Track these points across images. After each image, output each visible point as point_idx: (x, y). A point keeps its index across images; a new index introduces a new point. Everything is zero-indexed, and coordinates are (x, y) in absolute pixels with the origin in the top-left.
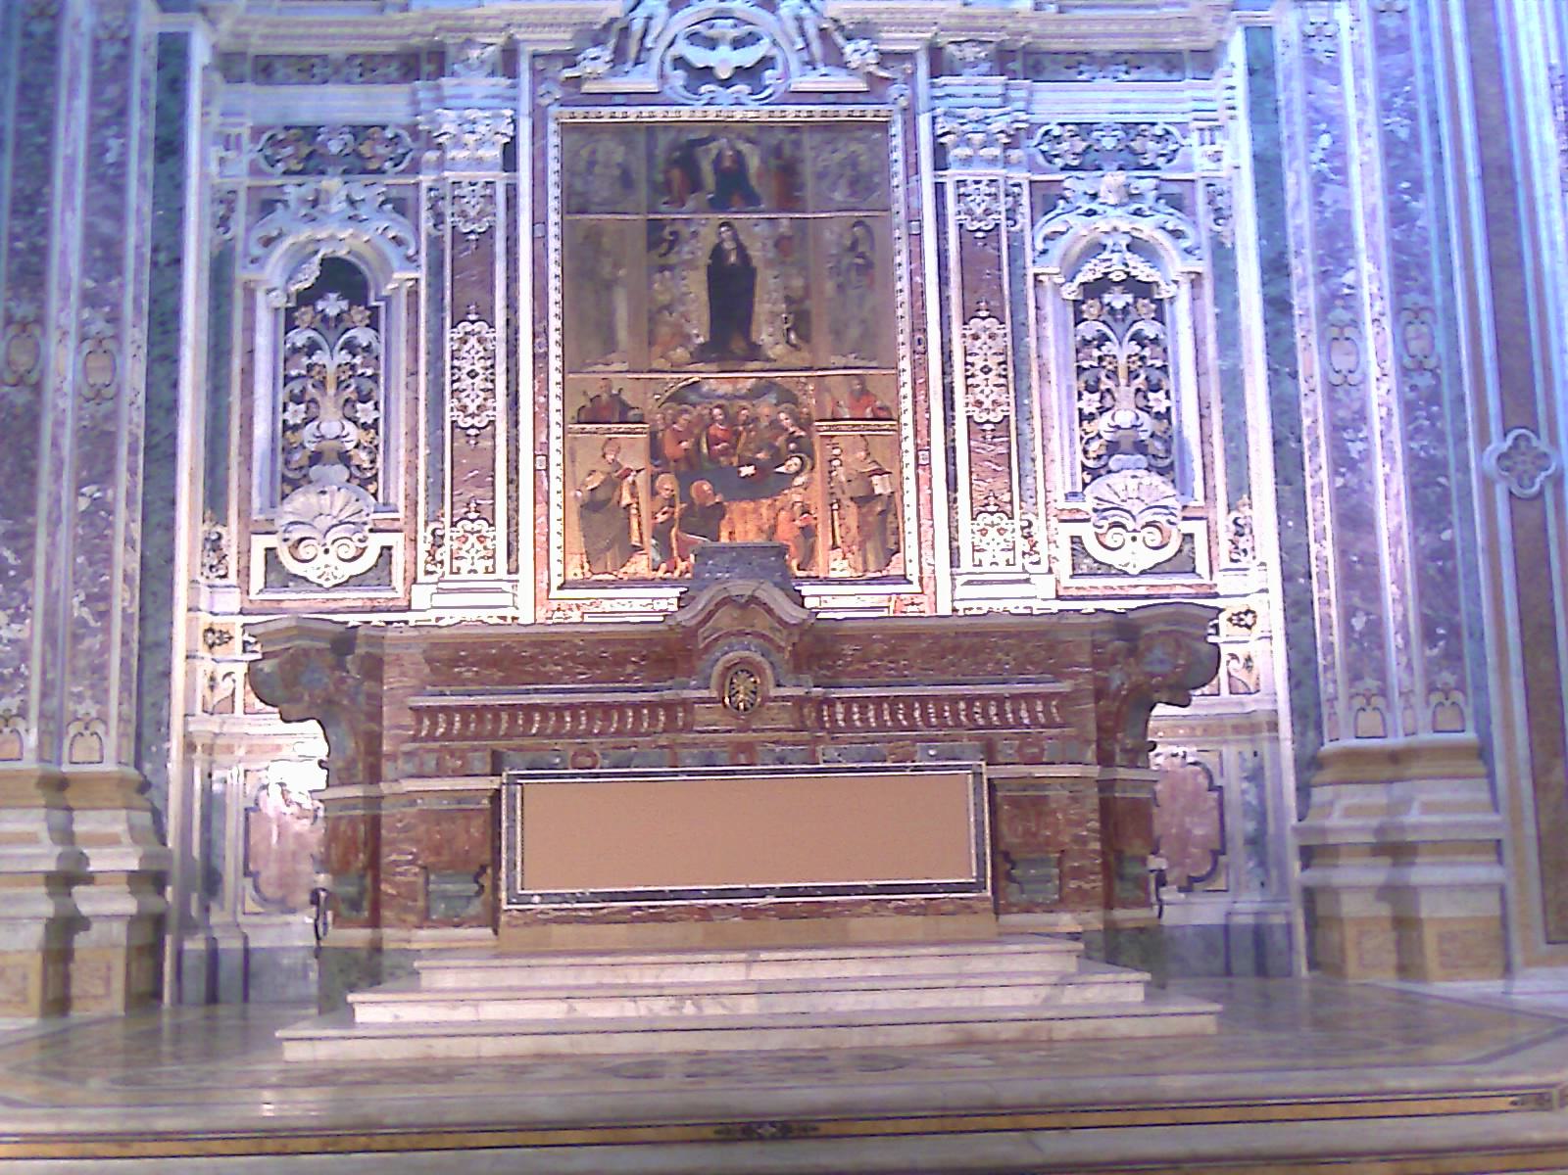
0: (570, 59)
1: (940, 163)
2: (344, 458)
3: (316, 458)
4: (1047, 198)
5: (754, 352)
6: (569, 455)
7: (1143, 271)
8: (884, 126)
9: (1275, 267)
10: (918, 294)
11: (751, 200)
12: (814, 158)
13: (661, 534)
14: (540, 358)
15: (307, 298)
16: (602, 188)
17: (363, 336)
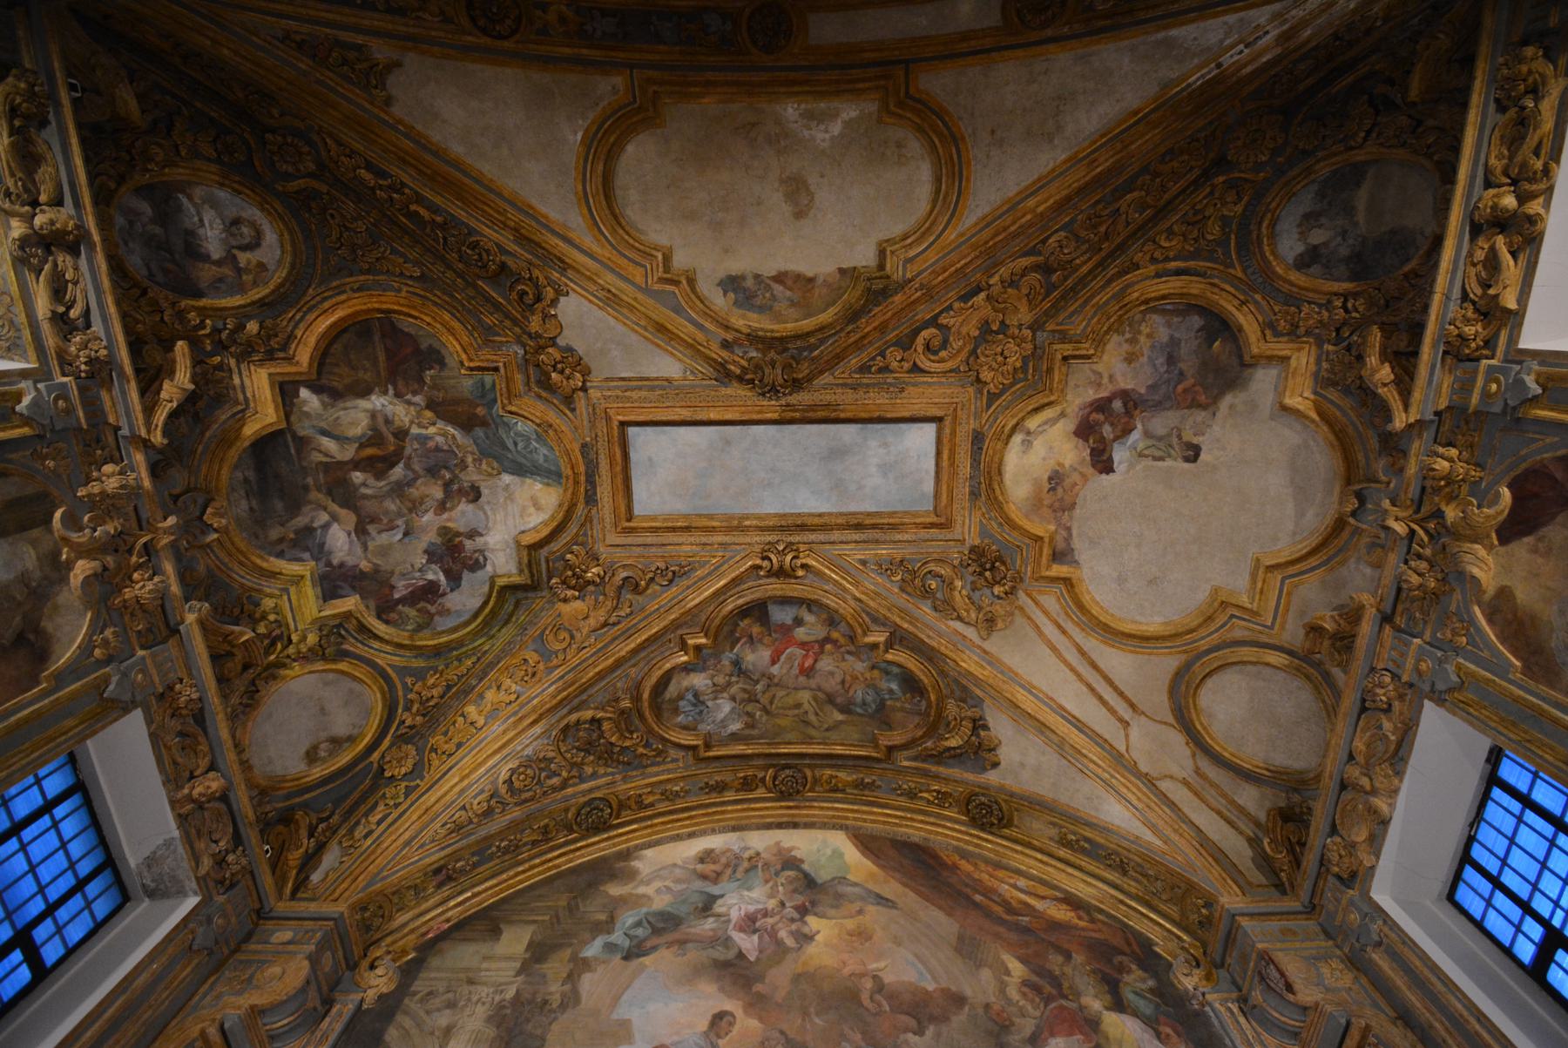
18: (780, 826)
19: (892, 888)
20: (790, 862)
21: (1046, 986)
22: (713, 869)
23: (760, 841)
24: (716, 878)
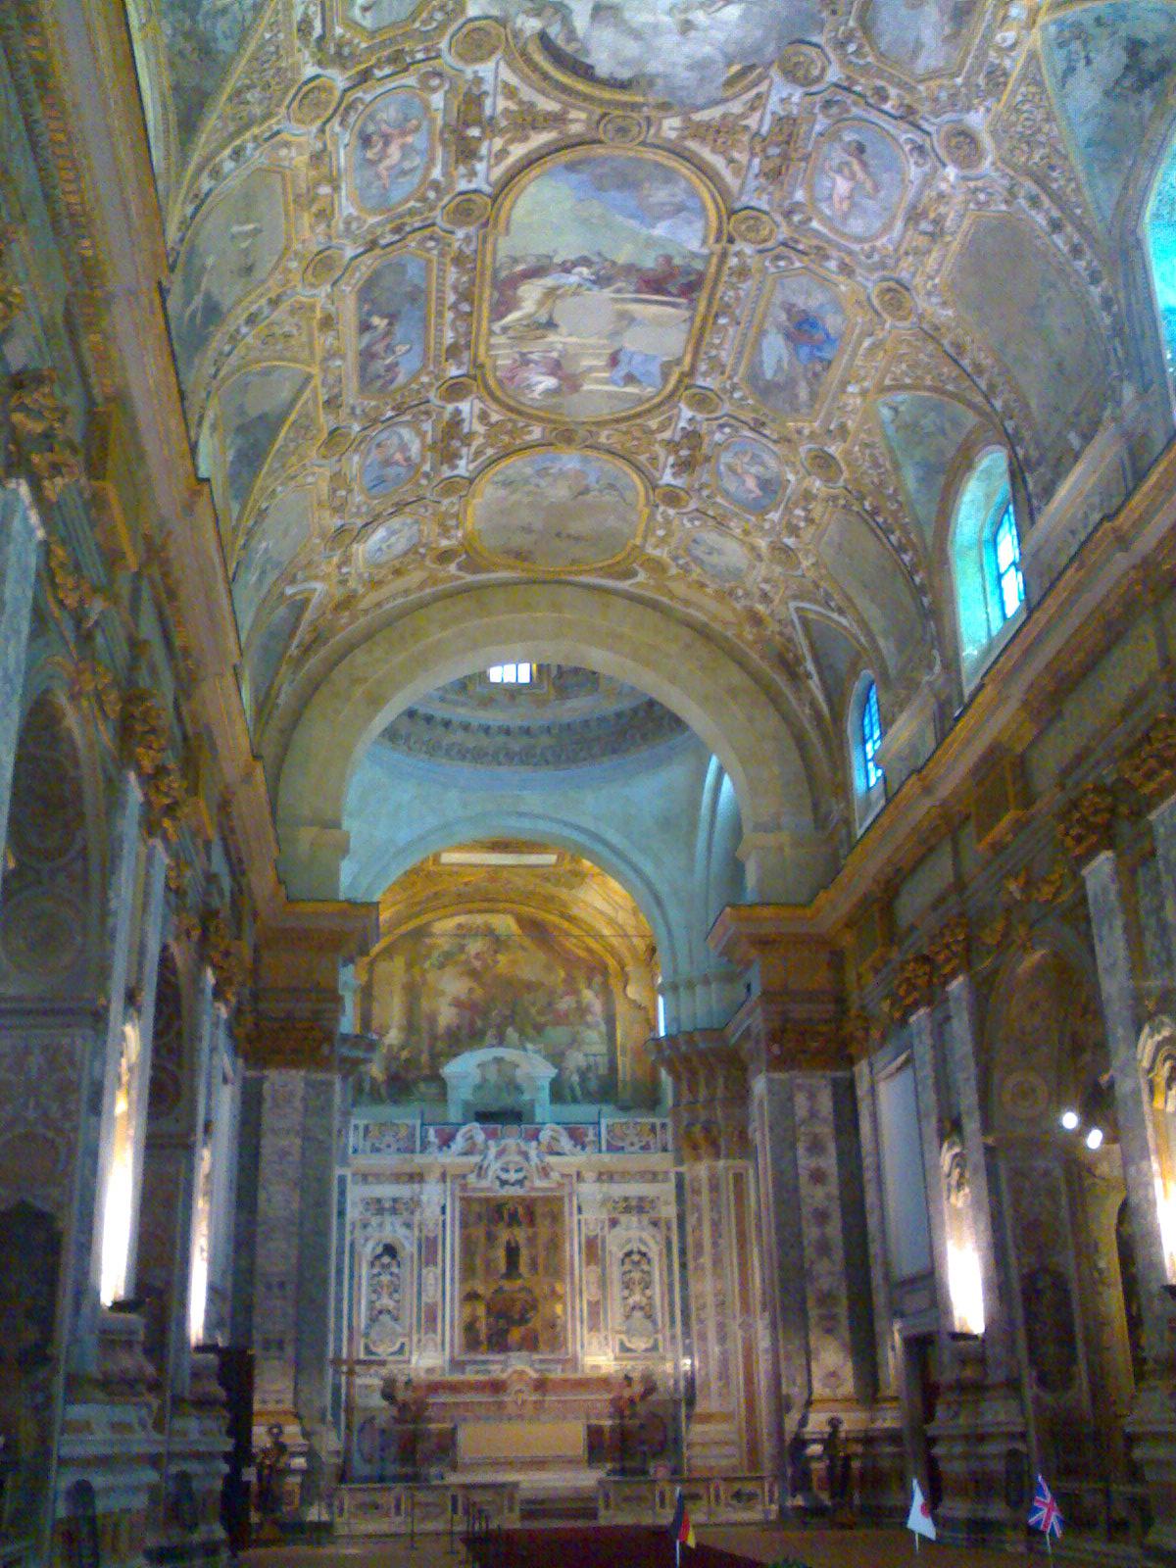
3: (380, 1312)
4: (614, 1223)
5: (520, 1276)
7: (644, 1249)
9: (683, 1252)
11: (519, 1224)
12: (539, 1210)
13: (489, 1338)
15: (378, 1257)
16: (472, 1219)
17: (395, 1270)
19: (527, 942)
20: (489, 932)
21: (570, 980)
22: (463, 933)
23: (479, 920)
24: (464, 936)
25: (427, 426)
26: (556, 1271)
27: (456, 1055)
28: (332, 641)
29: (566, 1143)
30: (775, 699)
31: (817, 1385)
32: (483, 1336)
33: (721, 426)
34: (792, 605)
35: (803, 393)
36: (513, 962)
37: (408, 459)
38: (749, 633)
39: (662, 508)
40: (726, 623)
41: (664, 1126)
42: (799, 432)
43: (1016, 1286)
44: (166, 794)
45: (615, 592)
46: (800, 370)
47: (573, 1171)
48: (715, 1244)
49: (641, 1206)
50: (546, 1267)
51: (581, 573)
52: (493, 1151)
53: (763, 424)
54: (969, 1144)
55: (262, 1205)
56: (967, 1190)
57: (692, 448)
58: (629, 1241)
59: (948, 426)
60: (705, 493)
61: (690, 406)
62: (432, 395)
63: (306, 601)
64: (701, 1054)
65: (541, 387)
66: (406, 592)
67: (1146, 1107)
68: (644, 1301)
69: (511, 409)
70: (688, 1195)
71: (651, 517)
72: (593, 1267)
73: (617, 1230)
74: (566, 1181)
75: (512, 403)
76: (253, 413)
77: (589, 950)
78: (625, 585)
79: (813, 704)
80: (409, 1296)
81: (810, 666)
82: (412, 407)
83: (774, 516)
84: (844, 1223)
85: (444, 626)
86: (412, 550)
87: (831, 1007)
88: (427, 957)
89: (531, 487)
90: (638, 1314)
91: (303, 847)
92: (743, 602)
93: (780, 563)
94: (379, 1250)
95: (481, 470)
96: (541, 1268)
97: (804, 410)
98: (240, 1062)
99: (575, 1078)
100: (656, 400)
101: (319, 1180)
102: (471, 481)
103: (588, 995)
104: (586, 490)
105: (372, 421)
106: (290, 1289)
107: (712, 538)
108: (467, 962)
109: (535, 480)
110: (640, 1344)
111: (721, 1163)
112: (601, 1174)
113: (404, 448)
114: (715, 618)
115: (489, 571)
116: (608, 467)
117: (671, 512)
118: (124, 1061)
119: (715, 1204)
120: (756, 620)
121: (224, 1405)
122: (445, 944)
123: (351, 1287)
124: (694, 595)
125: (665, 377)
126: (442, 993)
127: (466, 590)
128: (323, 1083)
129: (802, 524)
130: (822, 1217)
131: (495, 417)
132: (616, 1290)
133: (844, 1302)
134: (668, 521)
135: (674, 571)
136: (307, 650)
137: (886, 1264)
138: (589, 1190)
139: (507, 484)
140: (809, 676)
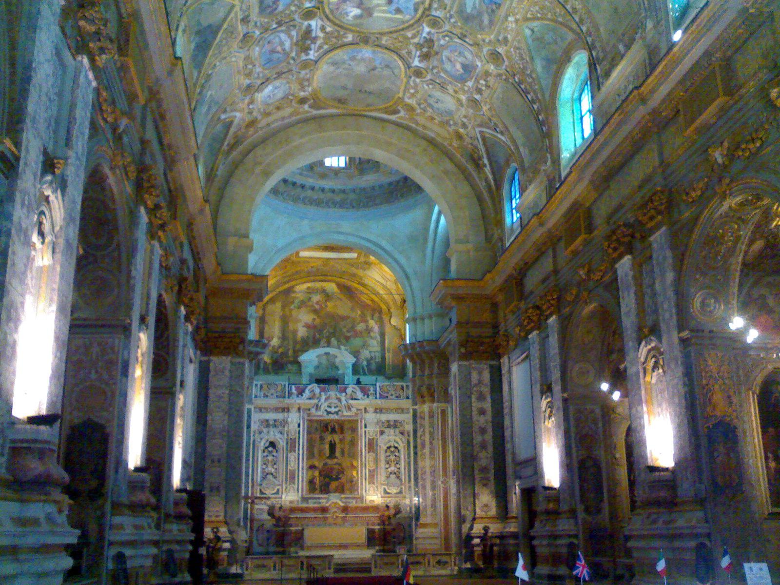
0: (309, 410)
1: (366, 427)
2: (272, 474)
3: (267, 474)
4: (382, 433)
5: (336, 457)
6: (307, 474)
7: (396, 445)
8: (357, 421)
9: (415, 447)
10: (361, 448)
12: (347, 426)
13: (321, 487)
14: (303, 459)
15: (266, 448)
17: (275, 454)
18: (322, 281)
19: (342, 296)
20: (324, 291)
22: (310, 291)
23: (318, 285)
25: (294, 33)
26: (353, 455)
27: (306, 351)
28: (245, 143)
29: (359, 395)
30: (468, 178)
31: (478, 511)
32: (317, 486)
33: (444, 37)
34: (478, 130)
35: (486, 22)
36: (336, 306)
37: (284, 50)
38: (456, 144)
39: (413, 78)
40: (445, 138)
41: (407, 386)
42: (484, 41)
43: (575, 464)
44: (160, 219)
45: (389, 121)
46: (485, 8)
47: (362, 408)
48: (431, 443)
49: (395, 425)
50: (349, 455)
51: (371, 111)
52: (323, 397)
53: (465, 36)
54: (555, 397)
55: (209, 422)
56: (553, 419)
57: (429, 48)
58: (389, 441)
59: (559, 40)
60: (435, 71)
61: (428, 25)
62: (296, 17)
63: (231, 122)
64: (428, 353)
65: (352, 14)
66: (283, 119)
67: (642, 381)
68: (396, 470)
69: (336, 25)
70: (418, 420)
71: (408, 82)
72: (371, 453)
73: (383, 437)
74: (359, 412)
75: (337, 22)
76: (205, 23)
77: (373, 301)
78: (393, 117)
79: (487, 180)
80: (281, 466)
81: (486, 161)
82: (285, 23)
83: (470, 84)
84: (494, 433)
85: (302, 137)
86: (285, 97)
87: (491, 330)
88: (293, 302)
89: (346, 66)
90: (393, 476)
91: (230, 248)
92: (453, 128)
93: (472, 107)
94: (268, 444)
95: (320, 58)
96: (346, 454)
97: (486, 30)
98: (198, 352)
99: (365, 363)
100: (411, 22)
101: (238, 411)
102: (316, 62)
103: (372, 323)
104: (374, 69)
105: (266, 29)
106: (223, 461)
107: (438, 94)
108: (312, 306)
109: (348, 62)
110: (394, 490)
111: (435, 405)
112: (376, 409)
113: (282, 43)
114: (438, 134)
115: (324, 108)
116: (386, 56)
117: (418, 80)
118: (139, 351)
119: (432, 425)
120: (460, 137)
121: (191, 518)
122: (301, 296)
123: (253, 462)
124: (428, 124)
125: (416, 10)
126: (299, 321)
127: (314, 118)
128: (239, 363)
129: (484, 88)
130: (483, 431)
131: (329, 29)
132: (382, 464)
133: (492, 472)
134: (416, 85)
135: (418, 111)
136: (232, 148)
137: (514, 454)
138: (370, 417)
139: (334, 64)
140: (485, 166)
